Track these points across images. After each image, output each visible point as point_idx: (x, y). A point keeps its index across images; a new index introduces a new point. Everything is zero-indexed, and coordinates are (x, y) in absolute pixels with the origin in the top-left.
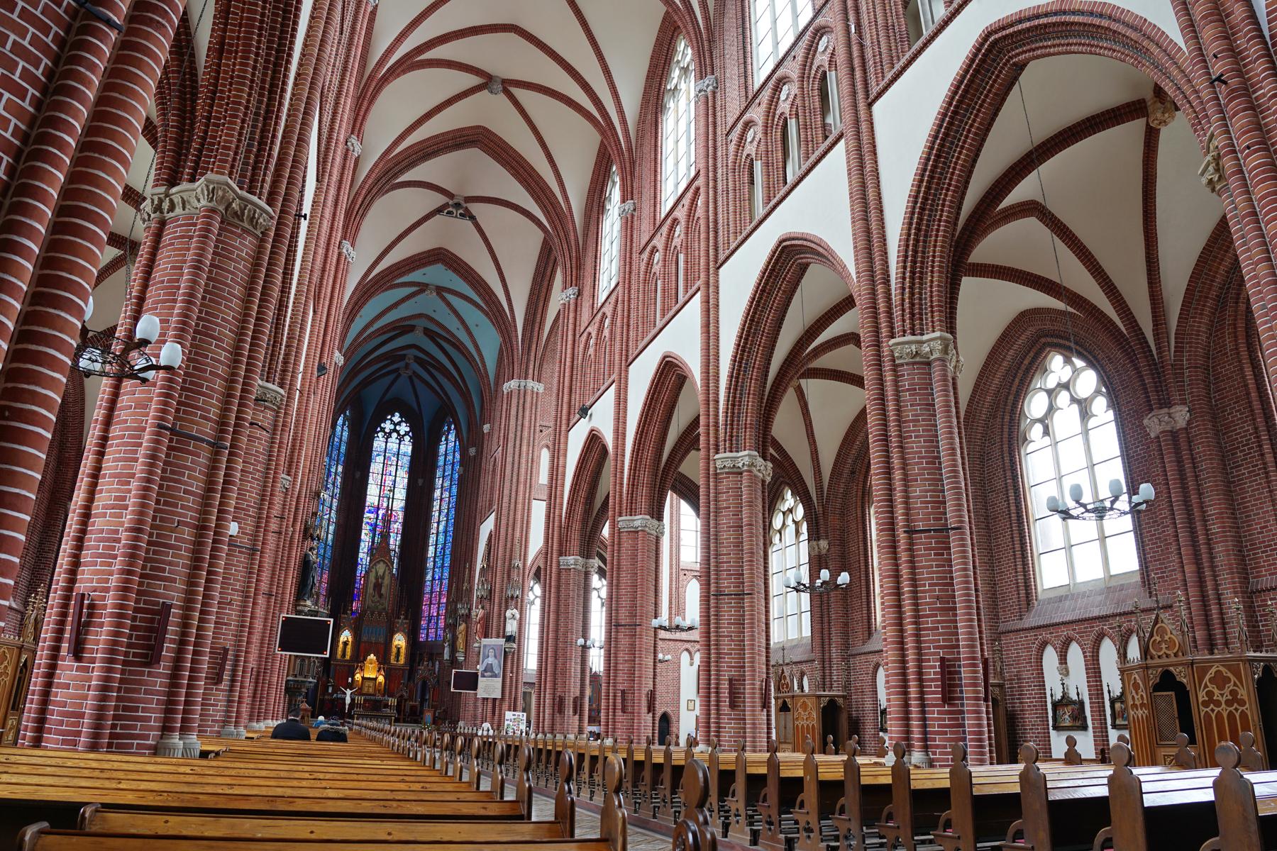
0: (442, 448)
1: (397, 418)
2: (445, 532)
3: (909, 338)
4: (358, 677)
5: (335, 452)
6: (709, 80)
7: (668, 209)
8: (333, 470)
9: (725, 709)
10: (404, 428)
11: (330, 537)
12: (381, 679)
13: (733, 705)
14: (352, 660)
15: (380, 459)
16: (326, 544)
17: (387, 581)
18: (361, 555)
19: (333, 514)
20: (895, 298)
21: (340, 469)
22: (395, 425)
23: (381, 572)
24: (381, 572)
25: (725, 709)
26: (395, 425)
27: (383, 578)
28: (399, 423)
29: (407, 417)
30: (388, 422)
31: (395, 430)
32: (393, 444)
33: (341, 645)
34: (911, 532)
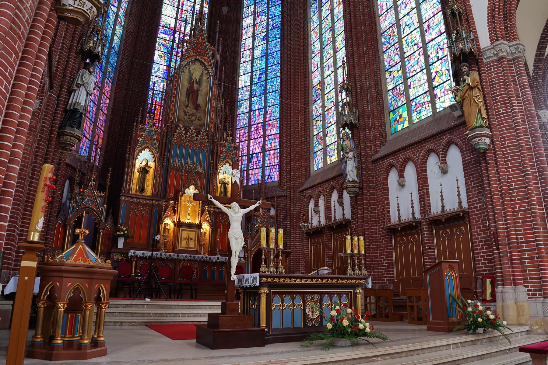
2: (266, 55)
4: (169, 222)
12: (206, 227)
14: (155, 196)
16: (111, 48)
18: (153, 79)
19: (121, 13)
23: (196, 76)
27: (199, 82)
33: (136, 174)
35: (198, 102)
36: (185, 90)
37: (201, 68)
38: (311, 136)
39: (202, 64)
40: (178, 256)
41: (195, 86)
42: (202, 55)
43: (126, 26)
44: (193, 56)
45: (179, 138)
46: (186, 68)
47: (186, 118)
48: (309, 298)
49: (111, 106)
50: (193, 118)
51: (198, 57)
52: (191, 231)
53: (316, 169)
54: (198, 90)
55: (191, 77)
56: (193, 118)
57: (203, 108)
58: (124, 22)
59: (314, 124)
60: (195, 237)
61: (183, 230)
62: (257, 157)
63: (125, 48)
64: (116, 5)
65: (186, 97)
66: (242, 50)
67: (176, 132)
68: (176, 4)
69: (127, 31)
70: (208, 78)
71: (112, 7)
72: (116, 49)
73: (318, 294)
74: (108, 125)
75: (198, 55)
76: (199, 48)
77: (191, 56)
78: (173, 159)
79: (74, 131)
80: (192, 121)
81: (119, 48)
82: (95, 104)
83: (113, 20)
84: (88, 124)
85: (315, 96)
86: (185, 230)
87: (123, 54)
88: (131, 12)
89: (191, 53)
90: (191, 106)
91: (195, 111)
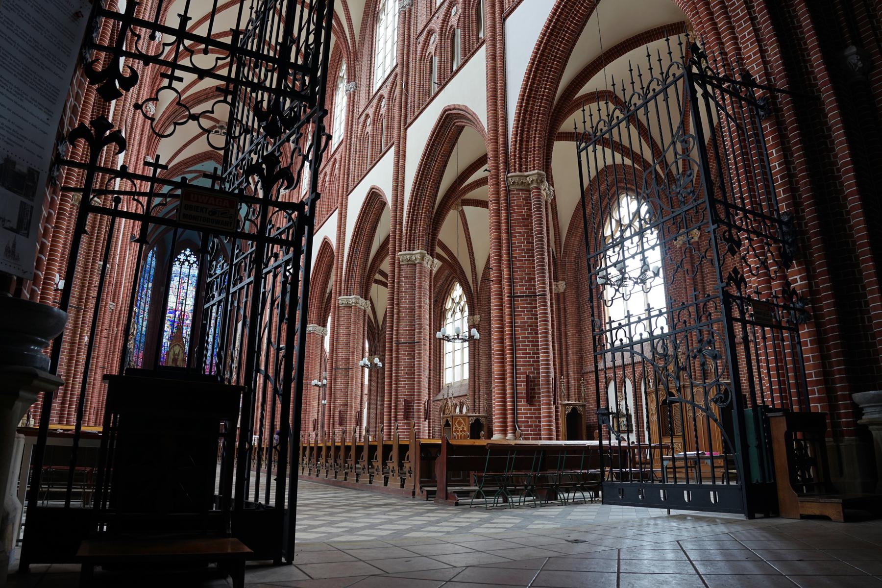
1: (188, 252)
3: (407, 252)
5: (147, 275)
6: (352, 84)
7: (336, 146)
8: (146, 286)
9: (337, 426)
10: (193, 259)
11: (144, 329)
13: (341, 424)
15: (177, 279)
17: (181, 357)
18: (164, 341)
19: (146, 315)
20: (404, 232)
21: (150, 285)
22: (187, 256)
24: (177, 352)
25: (337, 426)
26: (187, 256)
27: (178, 355)
28: (190, 256)
29: (195, 251)
31: (187, 260)
32: (185, 269)
34: (398, 343)
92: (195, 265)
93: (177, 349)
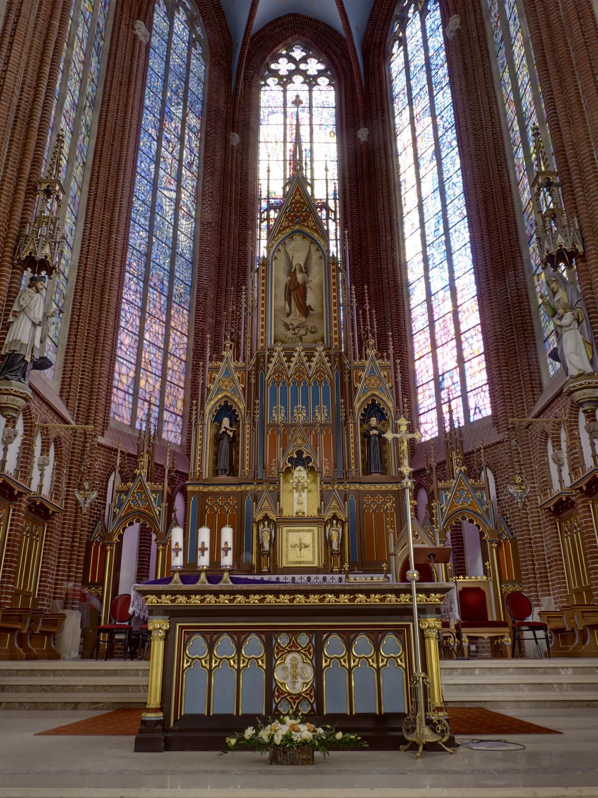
0: (397, 64)
17: (316, 276)
24: (299, 259)
27: (306, 270)
28: (304, 60)
30: (283, 61)
35: (308, 303)
36: (282, 288)
37: (307, 242)
38: (533, 308)
39: (305, 236)
40: (325, 579)
41: (300, 277)
42: (304, 221)
43: (199, 215)
44: (289, 226)
45: (279, 372)
46: (279, 250)
47: (290, 334)
48: (283, 640)
49: (192, 346)
50: (302, 332)
51: (297, 227)
52: (303, 531)
53: (552, 373)
54: (305, 283)
55: (289, 262)
56: (302, 332)
57: (317, 310)
58: (196, 210)
59: (537, 283)
60: (313, 541)
61: (290, 531)
62: (451, 378)
63: (202, 252)
64: (174, 187)
65: (286, 300)
66: (403, 193)
67: (271, 362)
68: (282, 154)
69: (202, 224)
70: (321, 257)
71: (166, 192)
72: (188, 256)
73: (308, 633)
74: (190, 377)
75: (297, 223)
76: (298, 211)
77: (285, 228)
78: (271, 409)
79: (11, 385)
80: (301, 338)
81: (193, 253)
82: (160, 348)
83: (171, 212)
84: (150, 381)
85: (529, 228)
86: (293, 531)
87: (201, 260)
88: (203, 191)
89: (285, 224)
90: (296, 312)
91: (303, 319)
92: (323, 81)
93: (298, 250)
